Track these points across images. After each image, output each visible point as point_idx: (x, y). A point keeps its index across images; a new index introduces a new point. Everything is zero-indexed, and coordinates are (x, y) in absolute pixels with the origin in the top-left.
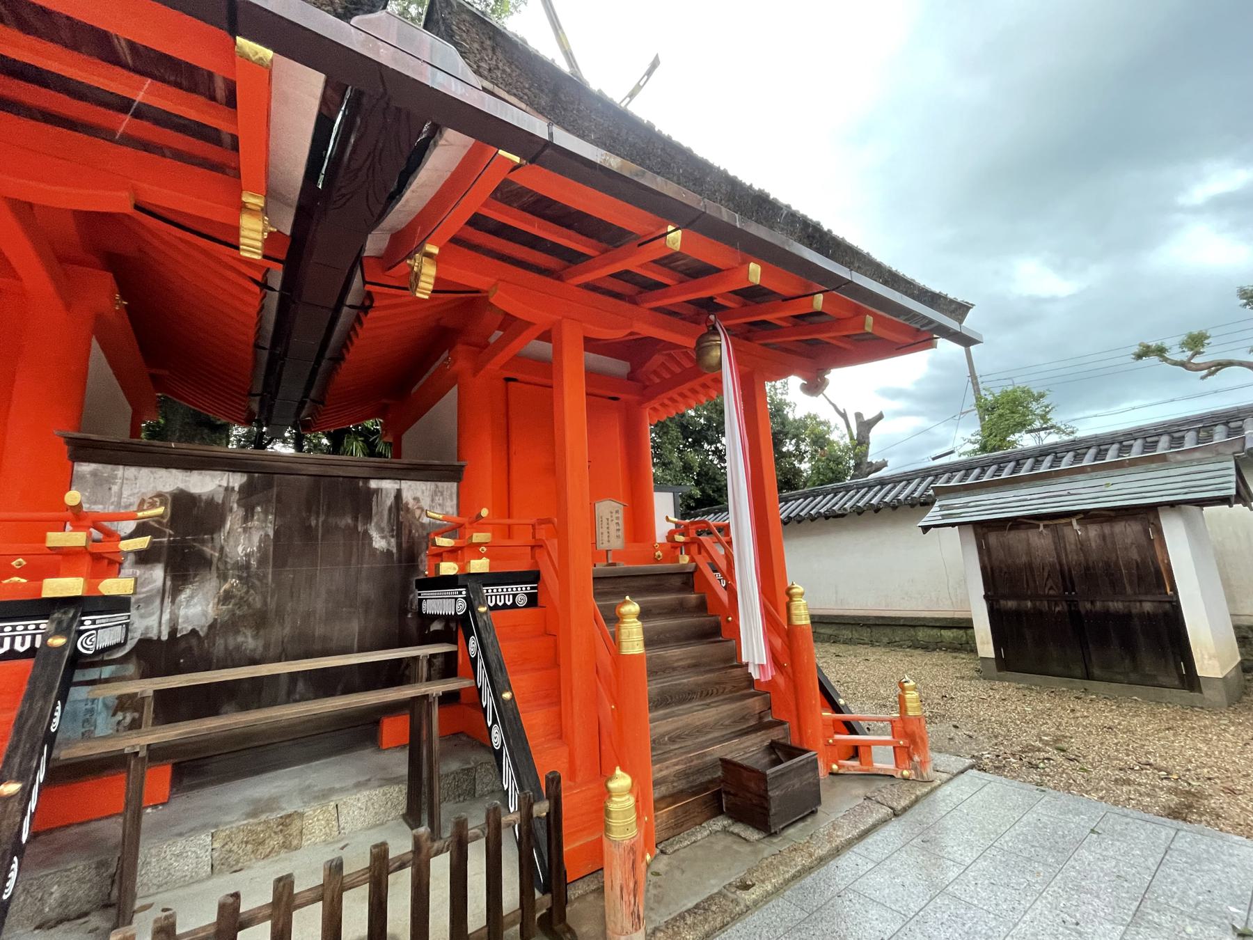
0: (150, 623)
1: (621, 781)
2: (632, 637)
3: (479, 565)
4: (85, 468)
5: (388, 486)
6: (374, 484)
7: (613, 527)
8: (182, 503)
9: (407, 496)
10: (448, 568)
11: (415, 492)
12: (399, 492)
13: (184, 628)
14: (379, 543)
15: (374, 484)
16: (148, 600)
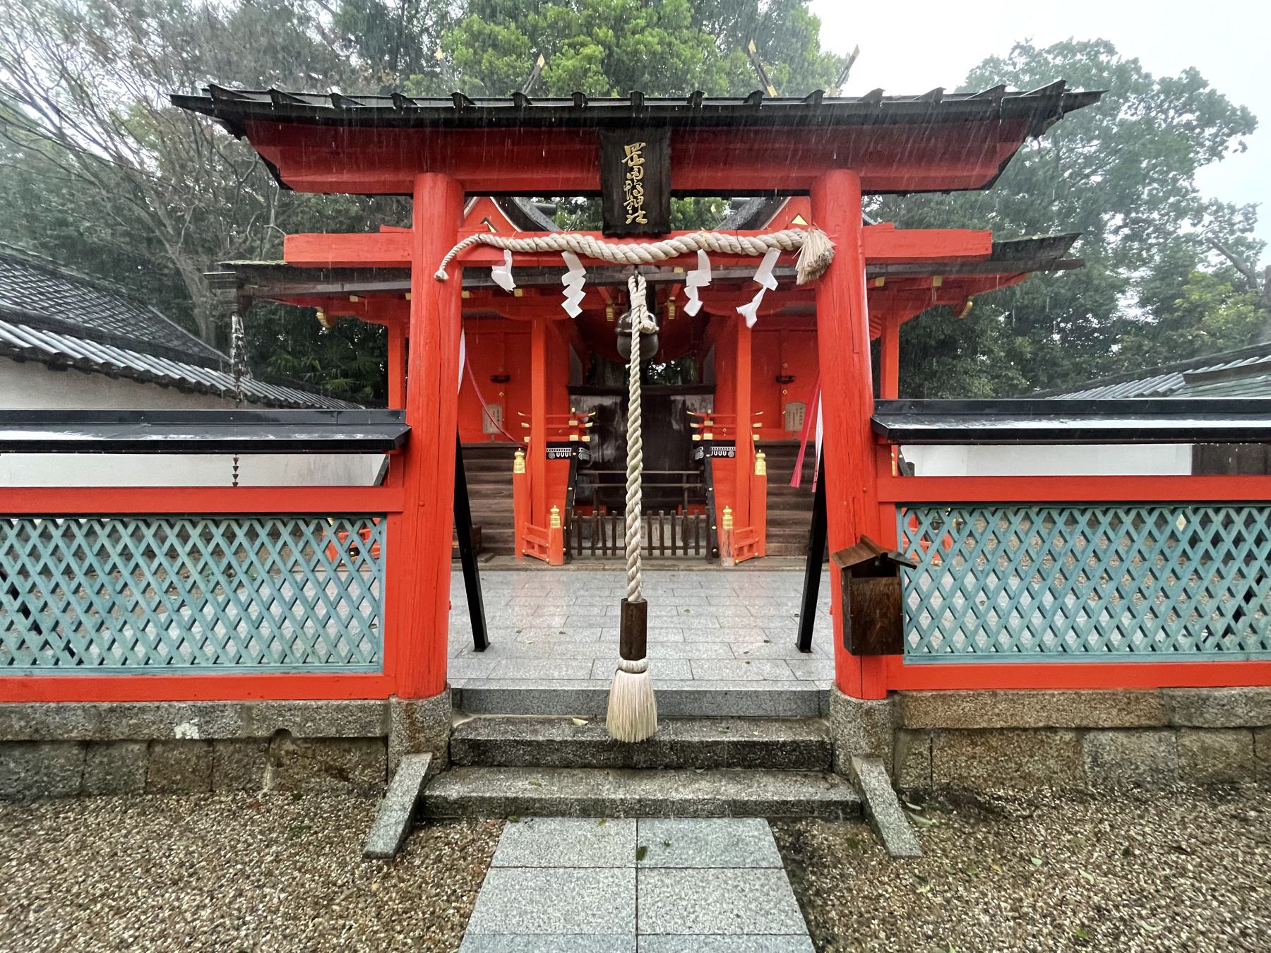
0: (596, 456)
1: (727, 510)
2: (760, 468)
3: (708, 436)
4: (573, 397)
5: (679, 398)
6: (672, 398)
7: (797, 418)
8: (601, 409)
9: (688, 404)
10: (696, 437)
11: (692, 400)
12: (684, 402)
13: (606, 459)
14: (676, 426)
15: (672, 398)
16: (594, 448)
